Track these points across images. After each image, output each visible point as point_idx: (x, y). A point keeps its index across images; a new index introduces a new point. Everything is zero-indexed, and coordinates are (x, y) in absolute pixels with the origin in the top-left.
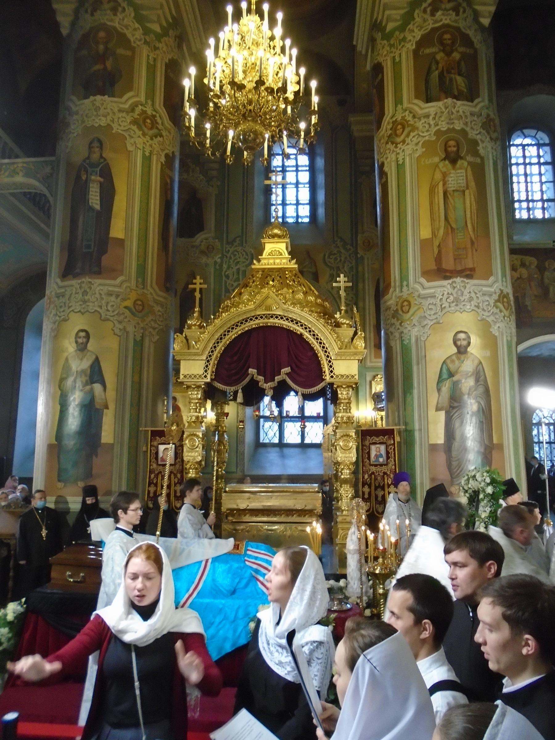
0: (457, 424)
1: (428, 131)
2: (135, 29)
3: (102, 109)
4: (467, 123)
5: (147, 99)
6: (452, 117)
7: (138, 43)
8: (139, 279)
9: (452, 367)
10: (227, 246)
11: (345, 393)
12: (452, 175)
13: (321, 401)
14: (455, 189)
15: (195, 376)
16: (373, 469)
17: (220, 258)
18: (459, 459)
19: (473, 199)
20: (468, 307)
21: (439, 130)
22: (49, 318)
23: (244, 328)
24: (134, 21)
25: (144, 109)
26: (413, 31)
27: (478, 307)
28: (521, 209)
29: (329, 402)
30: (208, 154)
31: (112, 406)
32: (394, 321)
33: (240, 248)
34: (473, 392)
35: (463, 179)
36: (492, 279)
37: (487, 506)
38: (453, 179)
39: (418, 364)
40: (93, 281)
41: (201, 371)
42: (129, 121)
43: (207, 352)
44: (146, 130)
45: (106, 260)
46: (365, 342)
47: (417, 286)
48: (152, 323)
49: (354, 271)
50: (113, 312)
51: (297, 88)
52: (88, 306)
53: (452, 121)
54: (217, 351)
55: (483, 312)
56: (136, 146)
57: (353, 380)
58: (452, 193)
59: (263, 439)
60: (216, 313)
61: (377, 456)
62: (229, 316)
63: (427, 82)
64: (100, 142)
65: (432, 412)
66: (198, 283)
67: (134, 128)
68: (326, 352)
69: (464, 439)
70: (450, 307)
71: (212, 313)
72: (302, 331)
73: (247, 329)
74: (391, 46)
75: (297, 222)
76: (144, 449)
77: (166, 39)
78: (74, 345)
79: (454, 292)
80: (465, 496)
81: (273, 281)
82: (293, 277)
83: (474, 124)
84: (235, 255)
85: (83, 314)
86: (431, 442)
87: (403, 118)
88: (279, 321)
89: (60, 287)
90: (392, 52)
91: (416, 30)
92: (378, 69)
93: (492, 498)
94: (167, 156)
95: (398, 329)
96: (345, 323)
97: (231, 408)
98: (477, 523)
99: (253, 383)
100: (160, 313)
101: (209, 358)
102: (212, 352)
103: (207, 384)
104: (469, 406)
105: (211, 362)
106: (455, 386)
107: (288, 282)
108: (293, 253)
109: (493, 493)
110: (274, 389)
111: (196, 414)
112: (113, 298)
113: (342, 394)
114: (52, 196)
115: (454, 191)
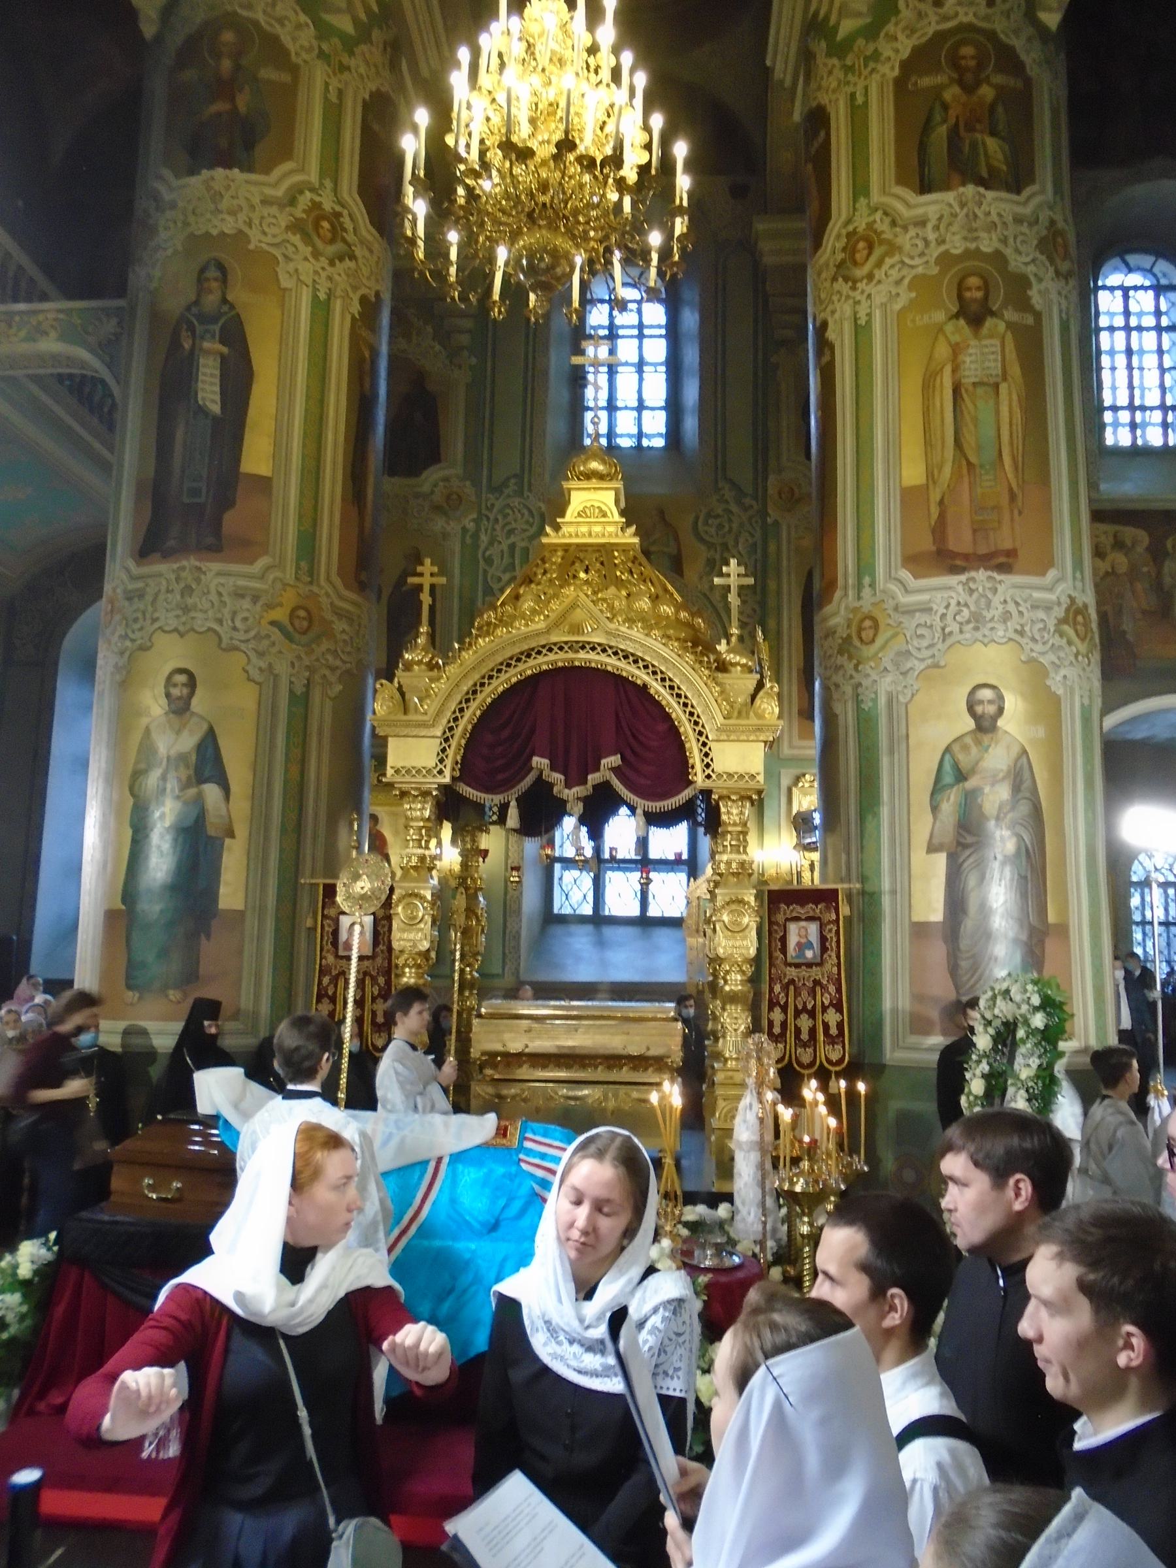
0: (972, 881)
1: (922, 254)
2: (299, 26)
3: (227, 197)
4: (1006, 237)
5: (322, 176)
6: (974, 225)
7: (305, 56)
8: (303, 564)
9: (964, 760)
10: (490, 496)
11: (735, 811)
12: (971, 351)
13: (682, 829)
14: (977, 380)
15: (419, 771)
16: (792, 972)
17: (474, 520)
18: (973, 956)
19: (1015, 403)
20: (1001, 633)
21: (947, 252)
22: (109, 642)
23: (524, 671)
24: (298, 8)
25: (317, 199)
26: (896, 39)
27: (1021, 633)
28: (1116, 424)
29: (701, 830)
30: (453, 298)
31: (241, 831)
32: (842, 660)
33: (516, 502)
34: (1006, 814)
35: (996, 360)
36: (1052, 574)
37: (1032, 1055)
38: (973, 358)
39: (891, 752)
40: (204, 565)
41: (431, 761)
42: (283, 224)
43: (445, 721)
44: (319, 244)
45: (231, 520)
46: (781, 705)
47: (893, 587)
48: (330, 657)
49: (759, 551)
50: (246, 632)
51: (643, 158)
52: (193, 618)
53: (975, 234)
54: (465, 719)
55: (1031, 645)
56: (299, 279)
57: (752, 784)
58: (971, 388)
59: (560, 906)
60: (464, 636)
61: (800, 946)
62: (493, 645)
63: (922, 148)
64: (222, 268)
65: (919, 855)
66: (427, 574)
67: (296, 239)
68: (696, 723)
69: (985, 911)
70: (961, 632)
71: (455, 634)
72: (646, 677)
73: (529, 672)
74: (848, 69)
75: (639, 447)
76: (309, 923)
77: (363, 48)
78: (164, 701)
79: (971, 601)
80: (986, 1032)
81: (587, 571)
82: (630, 564)
83: (1023, 242)
84: (506, 516)
85: (182, 635)
86: (915, 919)
87: (870, 226)
88: (597, 657)
89: (133, 578)
90: (848, 83)
91: (901, 37)
92: (818, 119)
93: (1044, 1039)
94: (364, 300)
95: (851, 677)
96: (738, 664)
97: (492, 840)
98: (1011, 1091)
99: (542, 787)
100: (346, 637)
101: (448, 734)
102: (456, 719)
103: (444, 788)
104: (999, 844)
105: (454, 743)
106: (970, 801)
107: (618, 573)
108: (631, 513)
109: (1046, 1026)
110: (586, 800)
111: (420, 851)
112: (246, 604)
113: (728, 812)
114: (118, 383)
115: (974, 384)
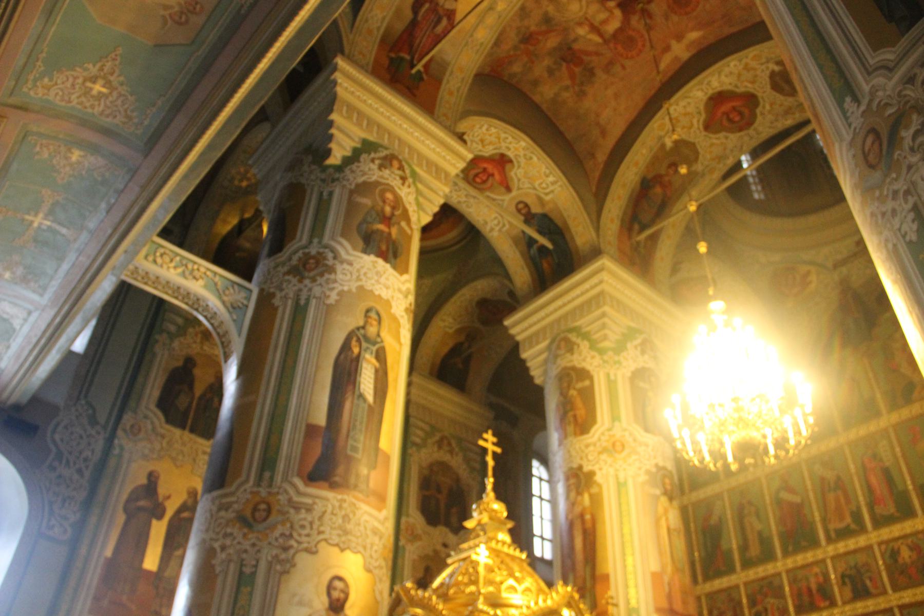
50: (377, 560)
52: (350, 540)
64: (378, 314)
74: (605, 362)
78: (325, 600)
